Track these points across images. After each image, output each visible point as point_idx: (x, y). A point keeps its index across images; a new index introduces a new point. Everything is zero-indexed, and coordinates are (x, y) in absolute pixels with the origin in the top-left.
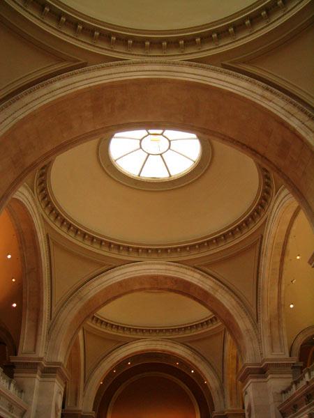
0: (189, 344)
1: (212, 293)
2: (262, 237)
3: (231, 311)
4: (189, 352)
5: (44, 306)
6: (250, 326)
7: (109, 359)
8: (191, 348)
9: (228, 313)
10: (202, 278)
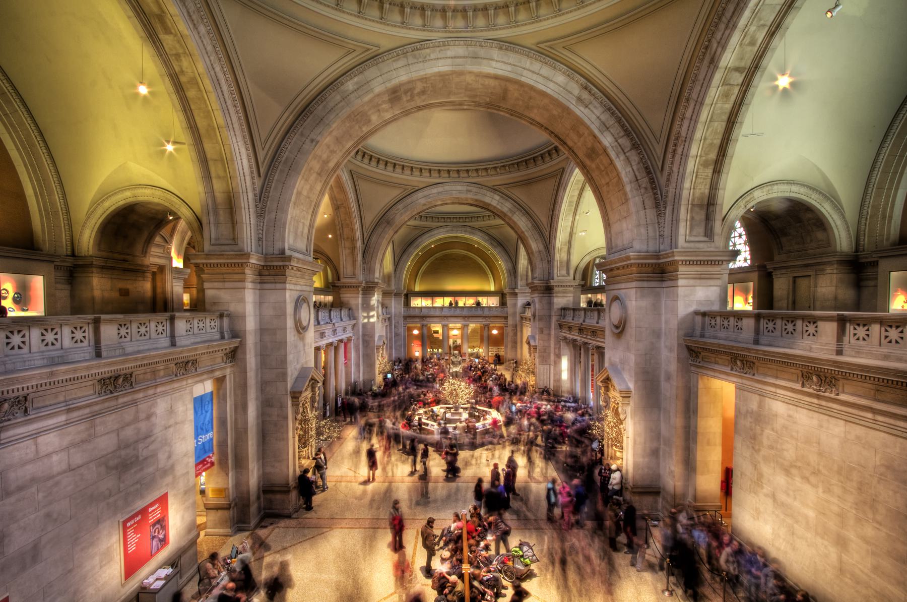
1: (509, 214)
2: (564, 169)
3: (526, 233)
4: (487, 238)
6: (541, 247)
9: (523, 232)
10: (502, 201)
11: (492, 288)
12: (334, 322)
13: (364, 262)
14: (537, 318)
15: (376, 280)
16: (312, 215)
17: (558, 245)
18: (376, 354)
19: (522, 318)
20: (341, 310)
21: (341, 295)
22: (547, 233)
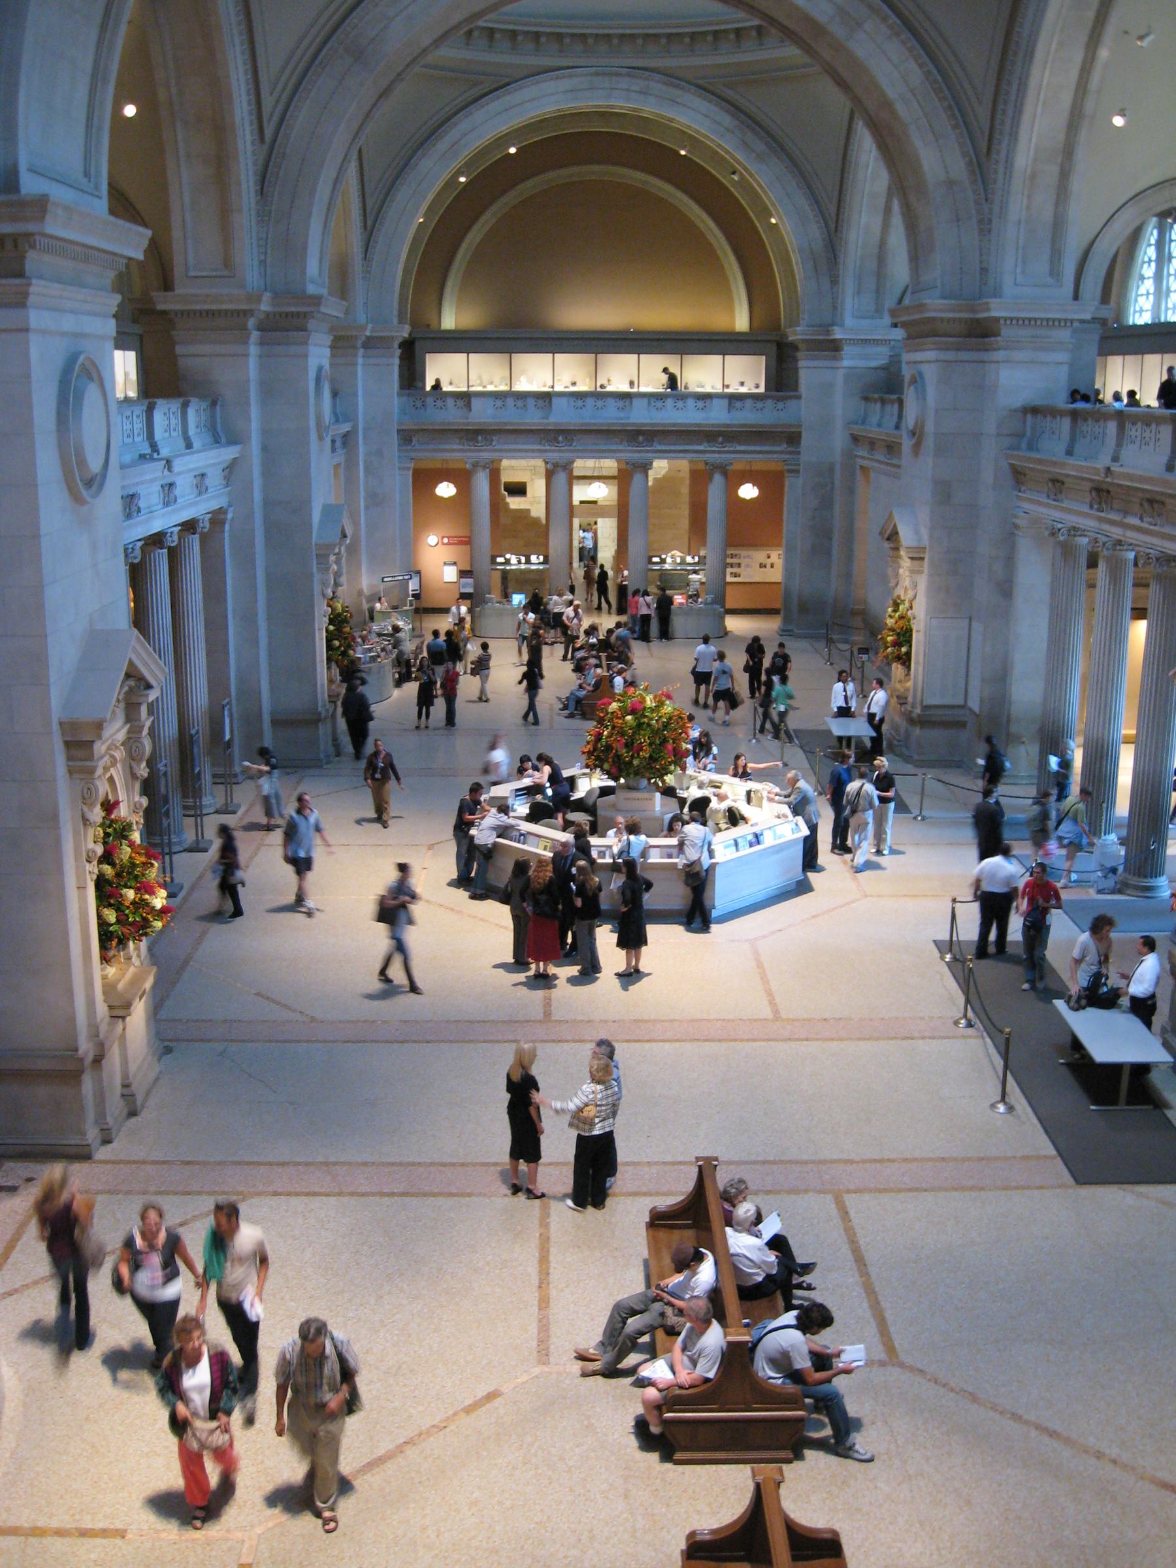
0: (729, 93)
3: (900, 108)
4: (727, 120)
5: (237, 112)
6: (959, 168)
7: (442, 145)
8: (735, 108)
9: (887, 104)
11: (742, 323)
12: (165, 452)
13: (264, 215)
14: (929, 443)
15: (311, 289)
16: (103, 27)
17: (1023, 159)
18: (317, 577)
19: (855, 439)
20: (185, 406)
21: (179, 350)
22: (983, 113)
